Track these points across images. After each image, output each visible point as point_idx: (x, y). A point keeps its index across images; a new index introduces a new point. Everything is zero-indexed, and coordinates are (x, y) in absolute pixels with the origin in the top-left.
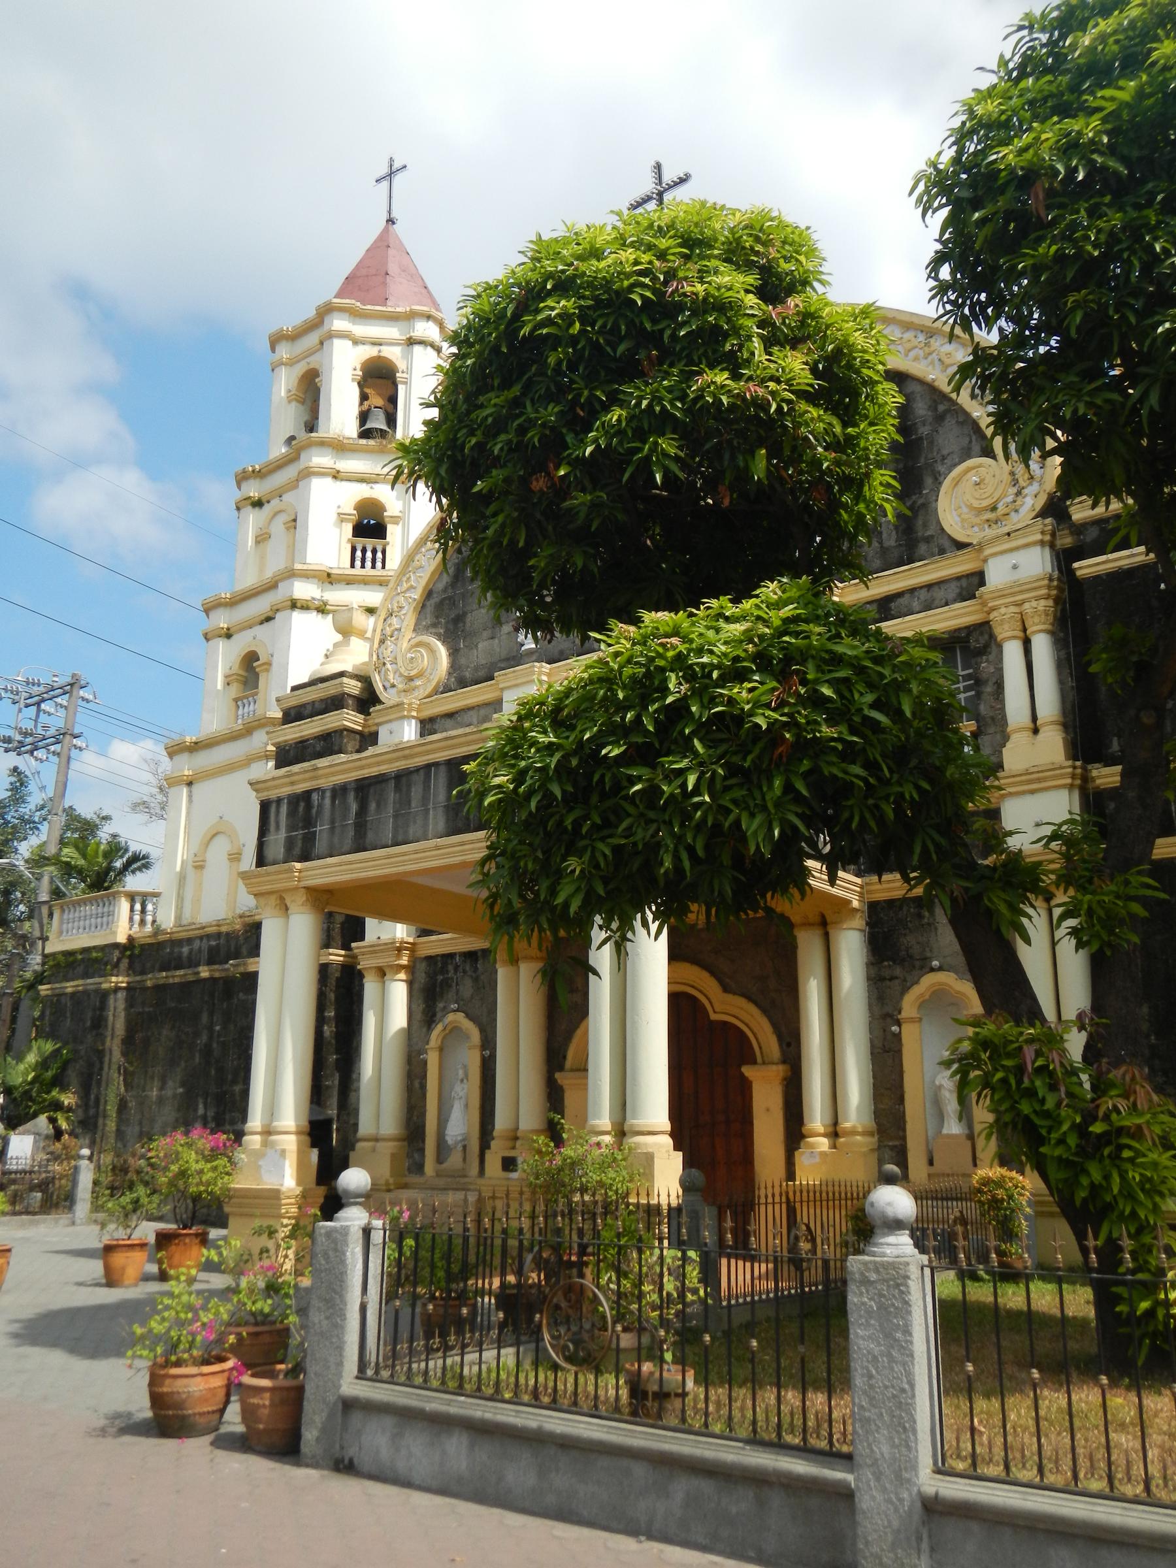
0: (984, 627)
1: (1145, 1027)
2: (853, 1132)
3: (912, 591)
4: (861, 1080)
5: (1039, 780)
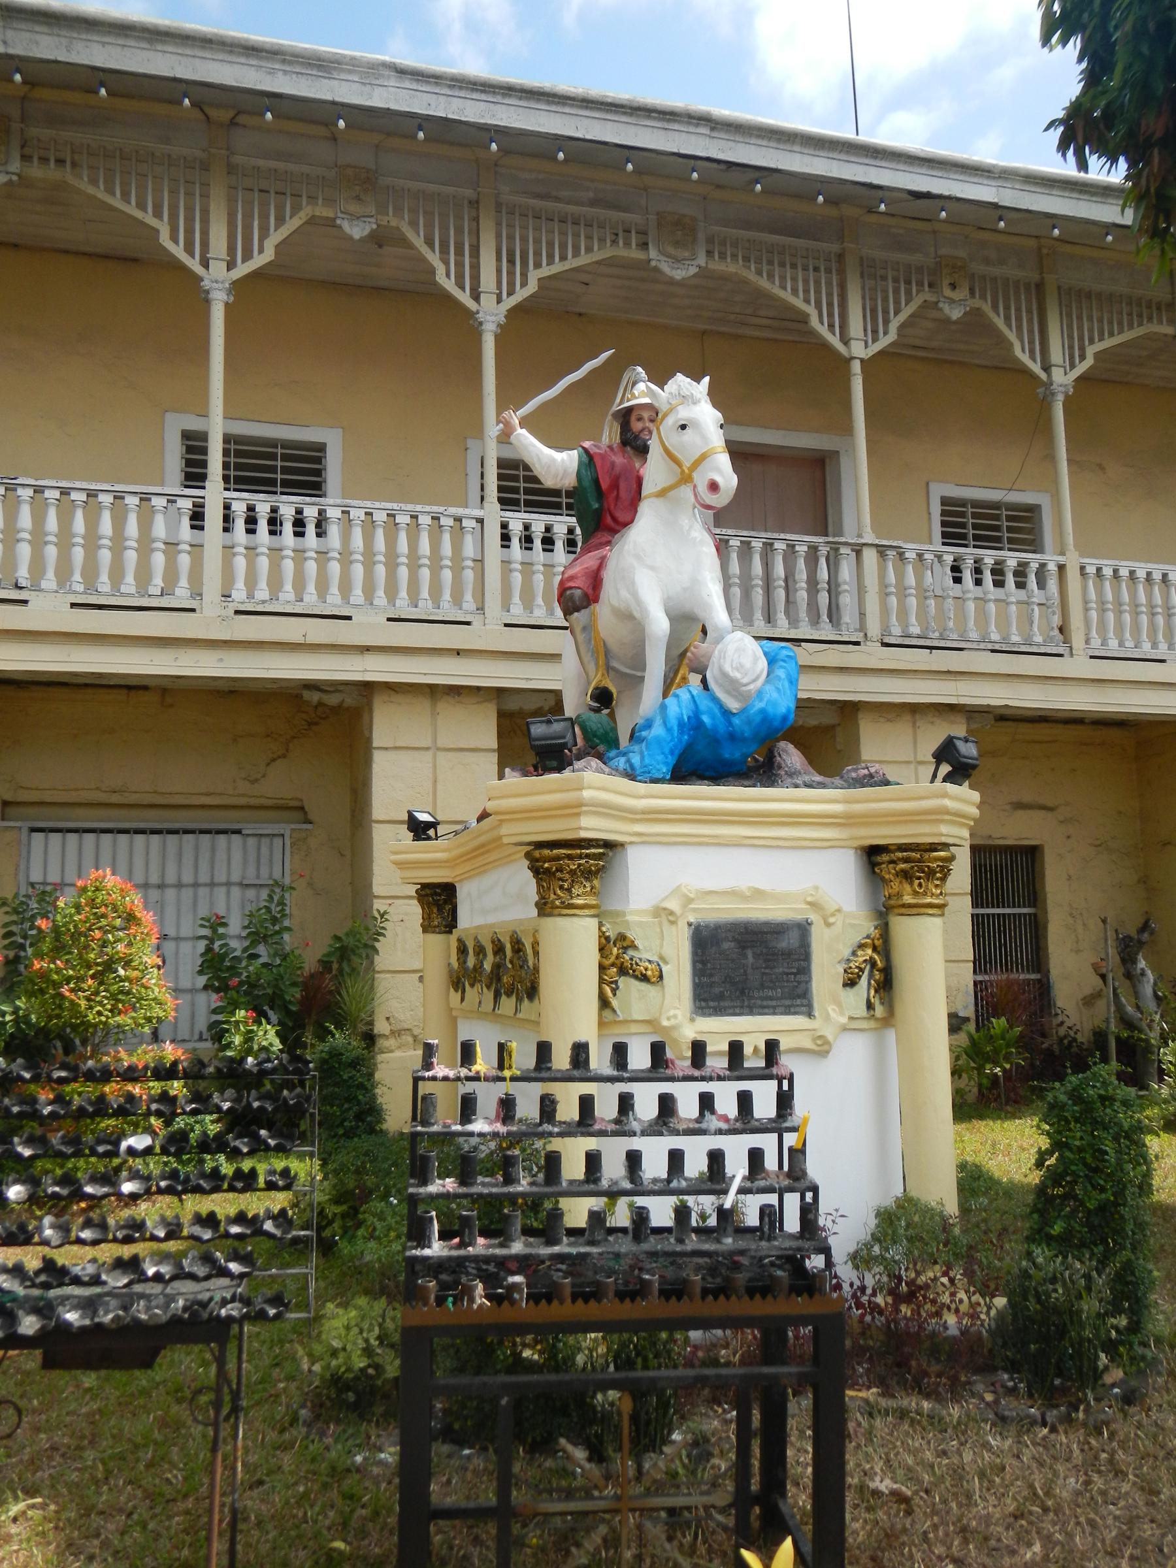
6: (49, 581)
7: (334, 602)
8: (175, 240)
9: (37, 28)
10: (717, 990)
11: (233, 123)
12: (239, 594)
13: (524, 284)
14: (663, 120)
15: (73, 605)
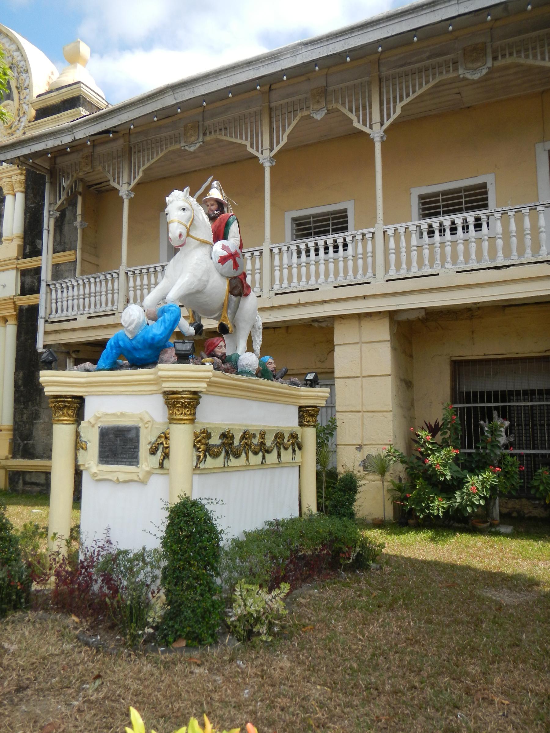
1: (20, 382)
5: (5, 265)
7: (312, 284)
10: (106, 454)
11: (270, 89)
12: (276, 287)
13: (394, 112)
14: (431, 7)
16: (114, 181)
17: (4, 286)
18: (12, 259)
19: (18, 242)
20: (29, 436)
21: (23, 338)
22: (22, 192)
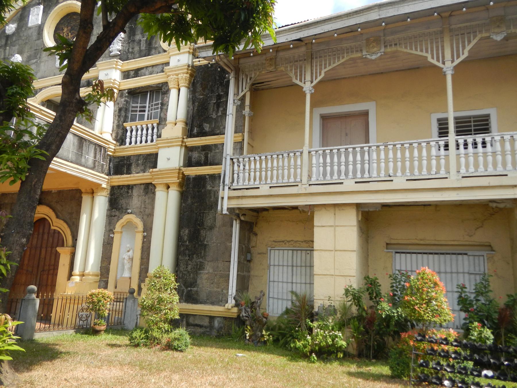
0: (166, 84)
1: (186, 238)
2: (89, 275)
3: (147, 67)
4: (95, 254)
5: (171, 142)
6: (399, 173)
7: (500, 170)
8: (433, 58)
9: (388, 8)
11: (450, 16)
12: (463, 171)
15: (407, 180)
16: (297, 79)
17: (169, 159)
18: (178, 138)
19: (180, 126)
20: (194, 284)
21: (189, 201)
22: (186, 87)
